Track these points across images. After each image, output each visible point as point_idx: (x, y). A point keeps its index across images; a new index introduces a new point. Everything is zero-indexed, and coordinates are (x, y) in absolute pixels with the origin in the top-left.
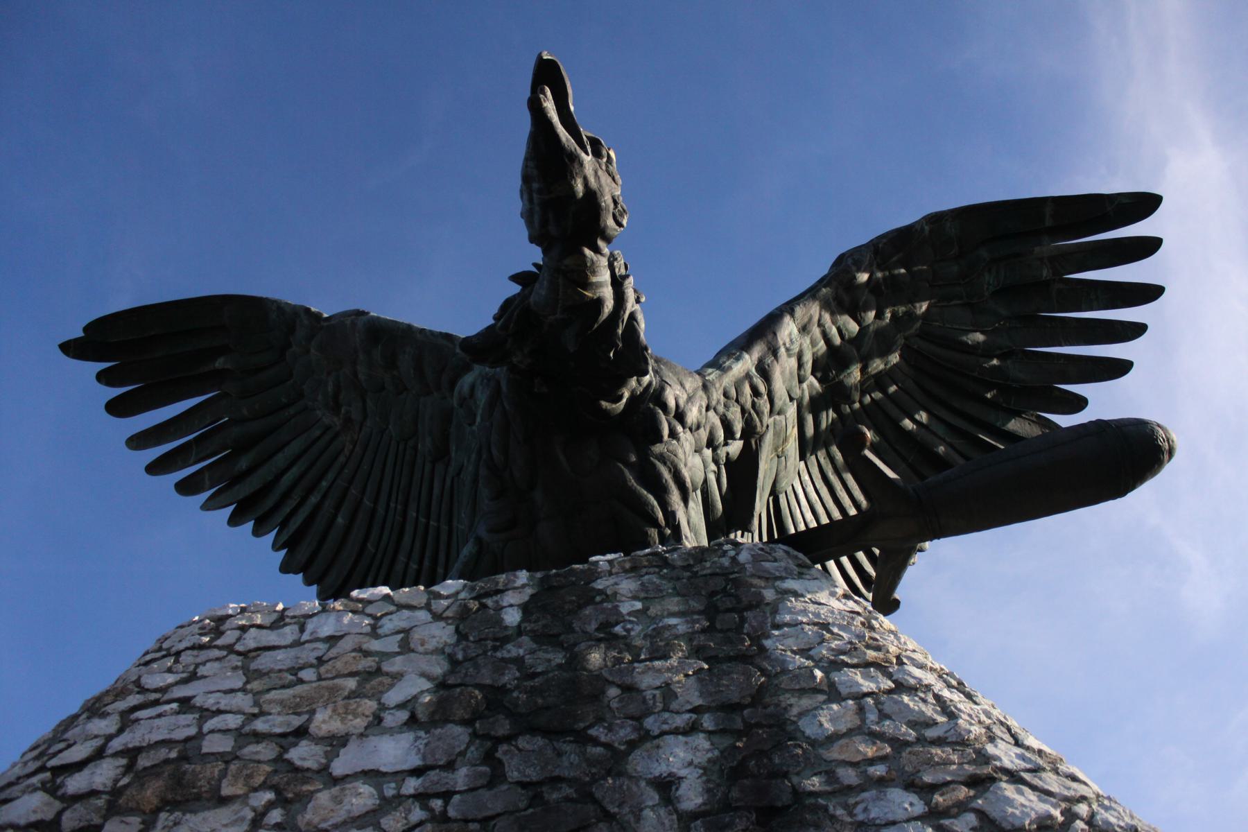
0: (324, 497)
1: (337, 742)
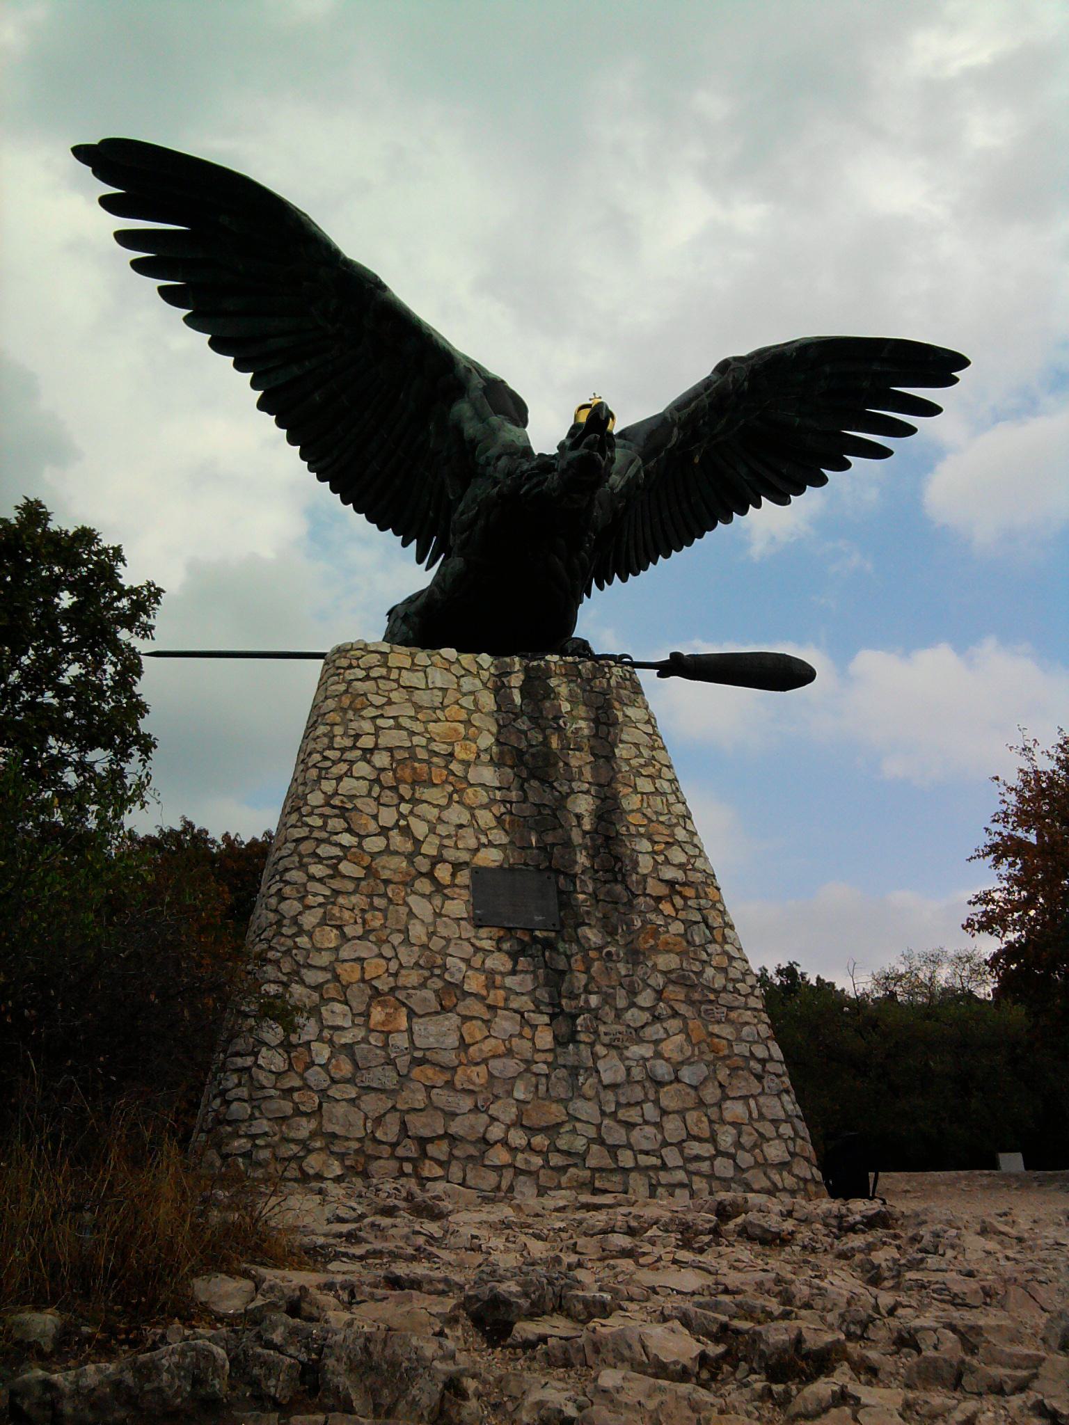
1: (466, 764)
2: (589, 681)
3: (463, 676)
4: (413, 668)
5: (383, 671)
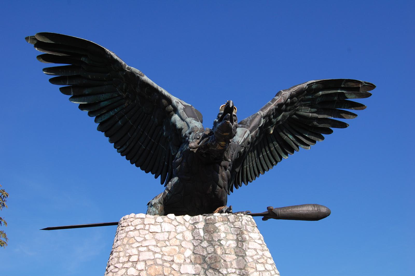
0: (115, 114)
1: (180, 265)
2: (233, 223)
3: (177, 225)
4: (156, 223)
5: (142, 226)
